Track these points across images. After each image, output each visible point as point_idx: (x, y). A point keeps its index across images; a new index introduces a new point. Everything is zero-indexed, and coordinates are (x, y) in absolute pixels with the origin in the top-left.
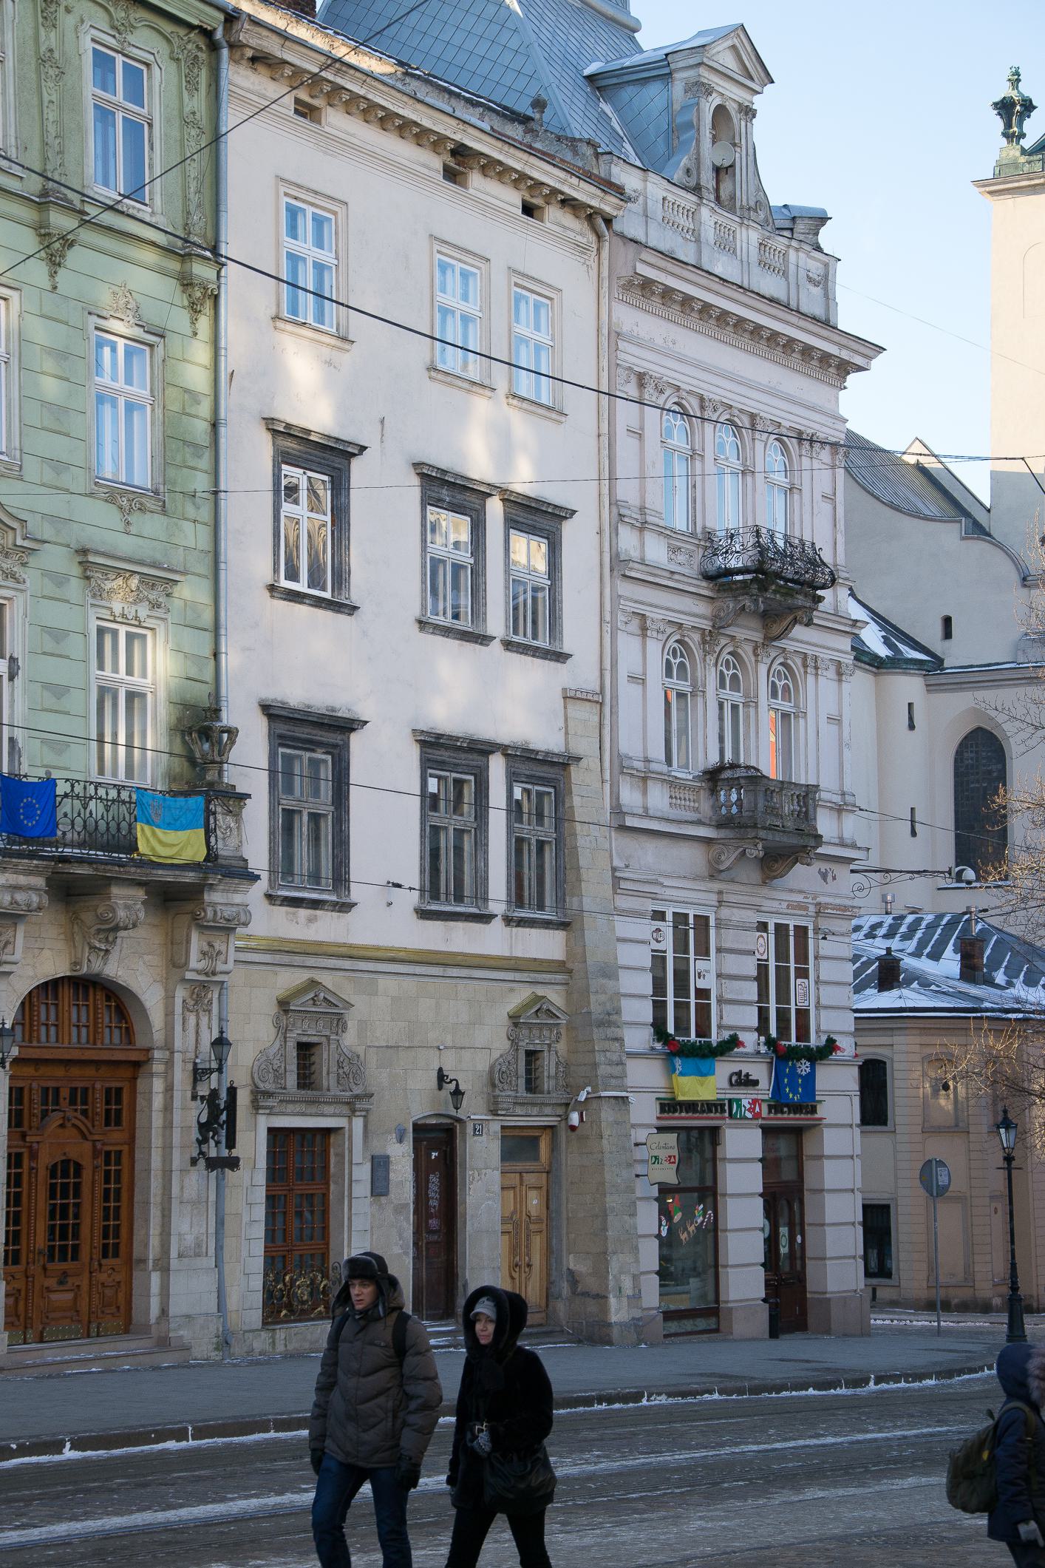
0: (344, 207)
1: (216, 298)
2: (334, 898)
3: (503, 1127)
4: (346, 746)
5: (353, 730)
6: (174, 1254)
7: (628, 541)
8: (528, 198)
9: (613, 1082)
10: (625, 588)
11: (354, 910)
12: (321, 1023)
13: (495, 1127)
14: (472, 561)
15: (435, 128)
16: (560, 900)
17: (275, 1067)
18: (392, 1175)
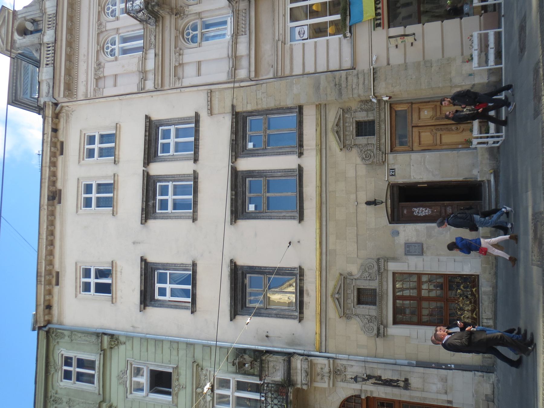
0: (78, 263)
1: (112, 336)
3: (392, 151)
4: (242, 267)
5: (235, 265)
6: (445, 397)
7: (150, 85)
8: (58, 153)
9: (366, 82)
10: (167, 87)
11: (303, 267)
12: (348, 292)
13: (391, 157)
14: (171, 182)
17: (367, 322)
18: (414, 240)
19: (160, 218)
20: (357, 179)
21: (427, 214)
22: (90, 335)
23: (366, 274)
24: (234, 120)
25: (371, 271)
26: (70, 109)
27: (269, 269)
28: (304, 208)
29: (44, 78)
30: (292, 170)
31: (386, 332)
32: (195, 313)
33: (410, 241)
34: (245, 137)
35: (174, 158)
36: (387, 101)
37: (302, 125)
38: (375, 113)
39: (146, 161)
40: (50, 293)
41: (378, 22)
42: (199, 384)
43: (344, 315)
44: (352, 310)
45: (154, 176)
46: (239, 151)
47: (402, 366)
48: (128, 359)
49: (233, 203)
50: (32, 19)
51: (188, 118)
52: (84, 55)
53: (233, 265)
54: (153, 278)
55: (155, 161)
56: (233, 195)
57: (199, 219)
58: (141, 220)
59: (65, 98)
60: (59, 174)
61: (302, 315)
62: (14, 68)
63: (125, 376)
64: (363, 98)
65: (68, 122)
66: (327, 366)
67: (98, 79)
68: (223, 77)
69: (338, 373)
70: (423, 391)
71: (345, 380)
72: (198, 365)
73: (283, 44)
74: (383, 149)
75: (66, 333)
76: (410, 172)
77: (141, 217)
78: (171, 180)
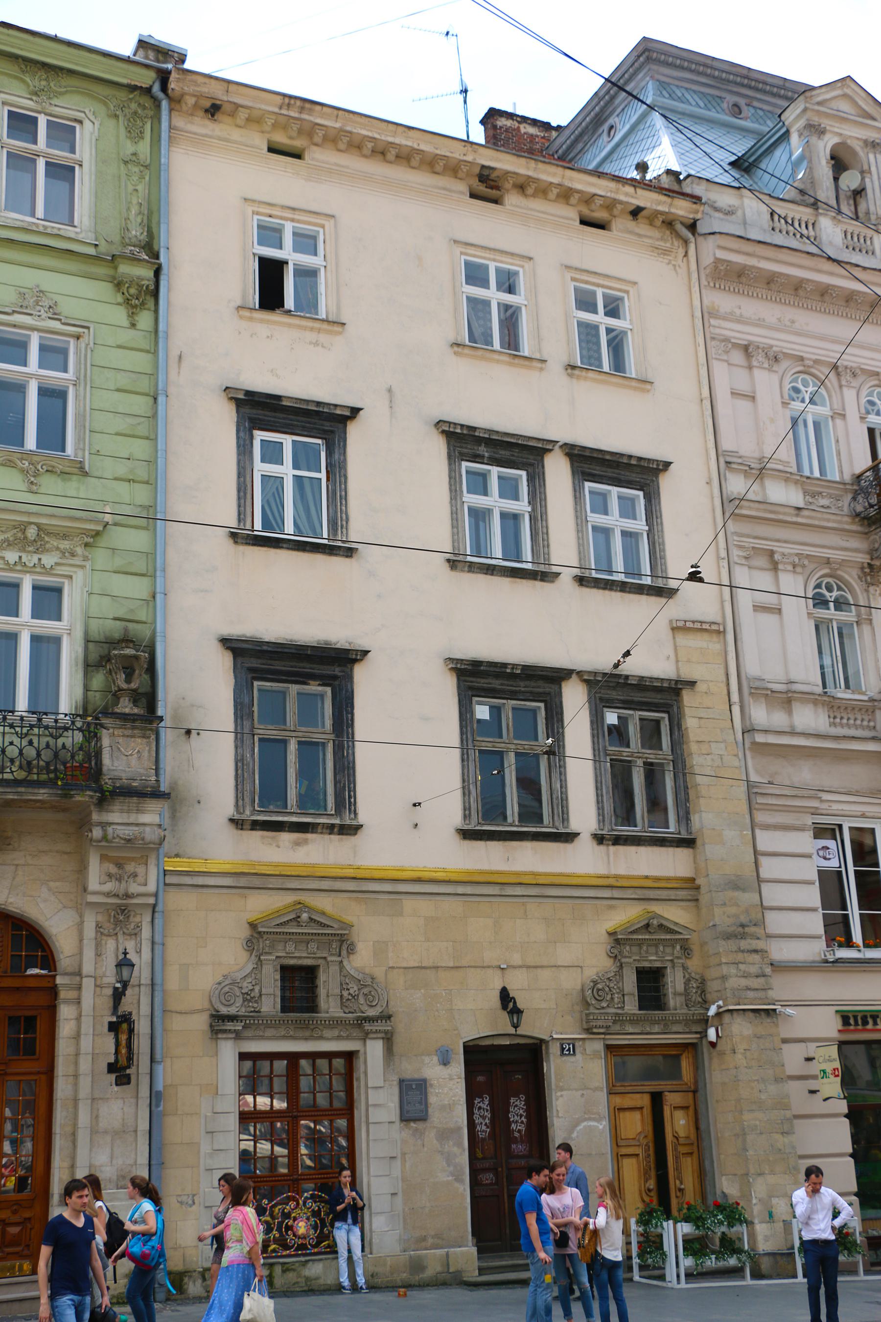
0: (332, 221)
1: (155, 294)
2: (337, 821)
3: (608, 1047)
4: (350, 678)
5: (355, 661)
7: (737, 485)
8: (586, 211)
9: (751, 994)
11: (359, 832)
12: (313, 946)
13: (599, 1046)
14: (529, 509)
15: (438, 152)
16: (685, 817)
18: (432, 1099)
19: (450, 470)
20: (553, 969)
21: (478, 1128)
22: (145, 221)
23: (354, 988)
24: (666, 685)
25: (362, 1000)
26: (680, 262)
27: (348, 747)
28: (488, 843)
29: (746, 201)
30: (565, 816)
31: (224, 1036)
32: (231, 541)
33: (430, 1090)
34: (625, 706)
35: (582, 522)
36: (704, 1034)
37: (656, 845)
38: (685, 1011)
39: (576, 452)
40: (254, 120)
41: (852, 1021)
42: (48, 534)
43: (260, 933)
44: (270, 953)
45: (543, 467)
46: (602, 691)
47: (148, 1077)
48: (91, 329)
49: (496, 667)
50: (864, 189)
51: (663, 567)
52: (793, 322)
53: (357, 655)
54: (305, 433)
55: (574, 473)
56: (513, 668)
57: (454, 573)
58: (450, 423)
59: (712, 260)
60: (537, 204)
61: (249, 827)
62: (723, 71)
63: (44, 315)
64: (713, 986)
65: (653, 251)
66: (142, 889)
67: (746, 349)
68: (752, 668)
69: (121, 918)
70: (94, 1131)
71: (102, 933)
72: (98, 534)
73: (812, 810)
74: (617, 1028)
75: (144, 148)
76: (569, 1090)
77: (457, 422)
78: (533, 510)
